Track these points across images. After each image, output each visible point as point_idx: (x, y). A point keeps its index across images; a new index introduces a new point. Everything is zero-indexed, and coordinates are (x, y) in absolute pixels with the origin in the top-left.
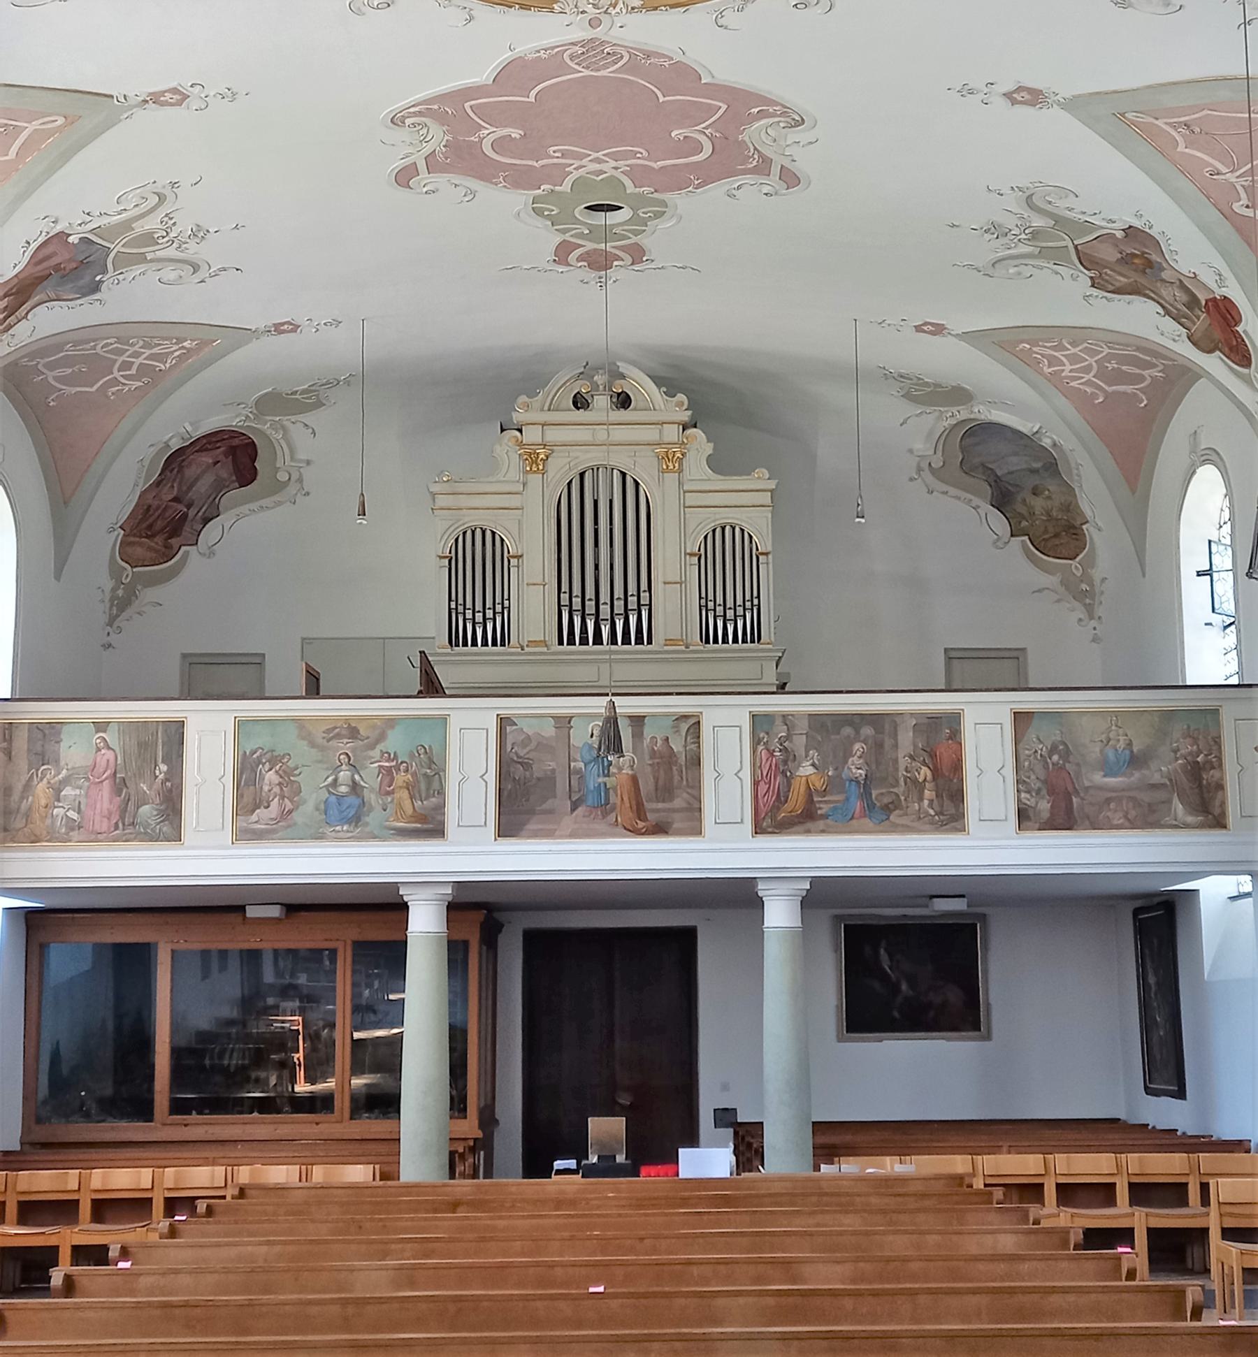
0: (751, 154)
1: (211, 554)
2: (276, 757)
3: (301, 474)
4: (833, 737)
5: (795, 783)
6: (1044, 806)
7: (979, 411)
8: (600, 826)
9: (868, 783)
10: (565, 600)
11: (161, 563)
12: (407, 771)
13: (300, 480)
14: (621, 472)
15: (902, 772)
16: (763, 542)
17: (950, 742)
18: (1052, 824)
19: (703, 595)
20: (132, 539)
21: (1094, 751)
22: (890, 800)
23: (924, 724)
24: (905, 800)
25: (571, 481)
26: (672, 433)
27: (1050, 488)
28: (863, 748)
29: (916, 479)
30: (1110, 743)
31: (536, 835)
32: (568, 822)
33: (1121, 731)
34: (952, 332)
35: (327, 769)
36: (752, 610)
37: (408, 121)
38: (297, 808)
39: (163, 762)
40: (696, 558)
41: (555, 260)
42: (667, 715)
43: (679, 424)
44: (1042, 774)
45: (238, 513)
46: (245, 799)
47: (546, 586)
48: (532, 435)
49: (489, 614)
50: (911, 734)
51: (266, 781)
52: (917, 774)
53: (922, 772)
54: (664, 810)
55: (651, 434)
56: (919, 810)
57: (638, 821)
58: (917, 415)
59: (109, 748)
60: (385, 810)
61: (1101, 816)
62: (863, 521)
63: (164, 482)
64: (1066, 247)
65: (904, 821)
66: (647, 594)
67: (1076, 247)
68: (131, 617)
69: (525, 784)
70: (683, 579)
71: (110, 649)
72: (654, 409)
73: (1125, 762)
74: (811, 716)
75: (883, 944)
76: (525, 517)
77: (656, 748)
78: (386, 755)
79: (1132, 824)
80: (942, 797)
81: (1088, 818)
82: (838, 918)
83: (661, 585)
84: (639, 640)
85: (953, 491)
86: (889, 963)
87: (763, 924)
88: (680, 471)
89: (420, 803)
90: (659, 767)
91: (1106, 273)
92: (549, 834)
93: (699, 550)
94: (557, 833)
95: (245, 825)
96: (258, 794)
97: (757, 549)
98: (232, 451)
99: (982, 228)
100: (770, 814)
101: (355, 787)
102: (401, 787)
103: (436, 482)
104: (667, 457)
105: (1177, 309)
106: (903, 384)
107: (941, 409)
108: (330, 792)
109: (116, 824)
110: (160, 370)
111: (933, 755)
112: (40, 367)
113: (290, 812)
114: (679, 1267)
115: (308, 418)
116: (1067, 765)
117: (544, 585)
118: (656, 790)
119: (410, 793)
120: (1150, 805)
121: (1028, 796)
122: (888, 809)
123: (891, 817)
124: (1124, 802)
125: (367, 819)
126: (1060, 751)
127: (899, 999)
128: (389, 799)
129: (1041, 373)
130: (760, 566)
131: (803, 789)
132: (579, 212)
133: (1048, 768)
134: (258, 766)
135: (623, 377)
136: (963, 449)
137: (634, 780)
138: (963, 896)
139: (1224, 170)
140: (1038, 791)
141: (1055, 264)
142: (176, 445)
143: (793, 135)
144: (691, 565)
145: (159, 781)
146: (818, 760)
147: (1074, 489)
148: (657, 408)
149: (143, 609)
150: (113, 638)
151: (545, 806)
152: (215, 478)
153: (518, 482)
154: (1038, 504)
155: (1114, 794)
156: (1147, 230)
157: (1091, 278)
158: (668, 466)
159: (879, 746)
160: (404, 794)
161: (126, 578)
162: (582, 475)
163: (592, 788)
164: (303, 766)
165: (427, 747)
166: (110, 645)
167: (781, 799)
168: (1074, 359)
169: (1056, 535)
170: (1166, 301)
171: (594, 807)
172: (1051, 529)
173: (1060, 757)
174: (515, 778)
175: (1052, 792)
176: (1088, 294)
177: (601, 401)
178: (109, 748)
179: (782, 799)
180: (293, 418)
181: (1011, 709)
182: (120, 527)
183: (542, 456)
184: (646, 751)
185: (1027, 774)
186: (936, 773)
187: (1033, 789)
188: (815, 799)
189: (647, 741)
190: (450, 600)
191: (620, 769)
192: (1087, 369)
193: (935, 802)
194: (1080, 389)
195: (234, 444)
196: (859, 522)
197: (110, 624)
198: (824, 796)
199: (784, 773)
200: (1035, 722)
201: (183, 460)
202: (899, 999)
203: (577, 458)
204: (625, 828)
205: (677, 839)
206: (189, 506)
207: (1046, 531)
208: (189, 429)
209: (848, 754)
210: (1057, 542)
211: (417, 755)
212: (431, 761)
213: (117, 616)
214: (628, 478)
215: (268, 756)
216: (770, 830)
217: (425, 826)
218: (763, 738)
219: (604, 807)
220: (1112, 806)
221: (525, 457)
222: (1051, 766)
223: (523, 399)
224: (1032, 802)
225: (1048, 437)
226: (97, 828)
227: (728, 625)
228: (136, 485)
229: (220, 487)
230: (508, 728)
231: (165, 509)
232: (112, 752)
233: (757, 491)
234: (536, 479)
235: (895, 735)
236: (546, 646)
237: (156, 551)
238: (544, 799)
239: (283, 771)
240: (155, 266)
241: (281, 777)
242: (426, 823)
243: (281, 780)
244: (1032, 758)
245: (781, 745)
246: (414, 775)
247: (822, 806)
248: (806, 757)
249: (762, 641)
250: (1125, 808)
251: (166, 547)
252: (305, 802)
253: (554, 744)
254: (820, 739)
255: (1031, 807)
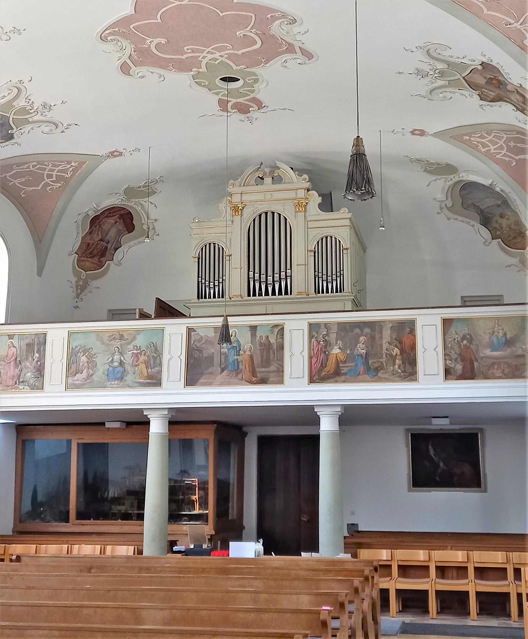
0: (280, 41)
1: (119, 264)
2: (86, 349)
3: (153, 225)
4: (349, 334)
5: (330, 357)
6: (459, 367)
7: (463, 176)
8: (234, 380)
9: (367, 356)
10: (251, 276)
11: (98, 269)
12: (145, 354)
13: (154, 229)
14: (278, 213)
15: (384, 351)
16: (346, 244)
17: (410, 335)
18: (463, 377)
19: (317, 270)
20: (83, 259)
21: (486, 338)
22: (378, 365)
23: (396, 326)
24: (386, 365)
25: (255, 219)
26: (301, 194)
27: (508, 214)
28: (365, 339)
29: (441, 213)
30: (494, 334)
31: (203, 384)
32: (219, 378)
33: (500, 328)
34: (429, 134)
35: (109, 355)
36: (340, 277)
37: (109, 38)
38: (95, 373)
39: (37, 352)
40: (313, 253)
41: (221, 110)
42: (268, 325)
43: (305, 189)
44: (458, 351)
45: (129, 245)
46: (72, 370)
47: (242, 269)
48: (236, 199)
49: (216, 284)
50: (389, 331)
51: (82, 361)
52: (392, 352)
53: (395, 351)
54: (265, 372)
55: (292, 194)
56: (393, 370)
57: (253, 378)
58: (434, 181)
59: (14, 347)
60: (134, 374)
61: (489, 373)
62: (384, 229)
63: (93, 232)
64: (459, 79)
65: (386, 376)
66: (290, 271)
67: (464, 78)
68: (86, 294)
69: (199, 360)
70: (306, 263)
71: (78, 308)
72: (293, 183)
73: (502, 344)
74: (339, 324)
75: (431, 443)
76: (232, 236)
77: (262, 341)
78: (135, 347)
79: (507, 376)
80: (405, 363)
81: (482, 373)
82: (407, 430)
83: (296, 266)
84: (286, 293)
85: (460, 218)
86: (433, 453)
87: (320, 429)
88: (305, 211)
89: (150, 370)
90: (263, 351)
91: (485, 92)
92: (209, 384)
93: (315, 249)
94: (214, 384)
95: (72, 381)
96: (78, 367)
97: (343, 247)
98: (122, 216)
99: (414, 73)
100: (317, 373)
101: (121, 363)
102: (142, 362)
103: (192, 222)
104: (299, 205)
105: (521, 106)
106: (421, 165)
107: (446, 177)
108: (110, 366)
109: (16, 382)
110: (66, 177)
111: (400, 342)
112: (8, 177)
113: (92, 375)
114: (76, 609)
115: (151, 199)
116: (471, 346)
117: (241, 269)
118: (262, 362)
119: (146, 365)
120: (516, 366)
121: (450, 362)
122: (377, 370)
123: (379, 374)
124: (502, 364)
125: (126, 378)
126: (468, 338)
127: (439, 471)
128: (137, 368)
129: (480, 151)
130: (344, 255)
131: (334, 360)
132: (218, 82)
133: (461, 348)
134: (78, 353)
135: (278, 168)
136: (462, 197)
137: (251, 357)
138: (447, 417)
139: (512, 22)
140: (456, 360)
141: (459, 89)
142: (92, 214)
143: (296, 29)
144: (310, 256)
145: (35, 361)
146: (342, 346)
147: (517, 213)
148: (294, 182)
149: (92, 290)
150: (79, 304)
151: (210, 370)
152: (117, 229)
153: (230, 220)
154: (504, 222)
155: (496, 361)
156: (491, 63)
157: (479, 95)
158: (299, 209)
159: (373, 338)
160: (143, 366)
161: (83, 276)
162: (260, 216)
163: (231, 361)
164: (98, 353)
165: (154, 343)
166: (77, 307)
167: (323, 366)
168: (494, 143)
169: (515, 238)
170: (515, 103)
171: (232, 371)
172: (512, 235)
173: (468, 342)
174: (195, 357)
175: (463, 360)
176: (481, 104)
177: (268, 180)
178: (14, 347)
179: (324, 365)
180: (145, 200)
181: (441, 317)
182: (75, 253)
183: (240, 208)
184: (257, 343)
185: (450, 351)
186: (402, 351)
187: (453, 359)
188: (340, 365)
189: (258, 338)
190: (198, 277)
191: (245, 352)
192: (501, 148)
193: (402, 366)
194: (503, 159)
195: (122, 213)
196: (382, 229)
197: (78, 296)
198: (345, 364)
199: (325, 352)
200: (454, 324)
201: (100, 222)
202: (439, 471)
203: (257, 208)
204: (247, 381)
205: (271, 386)
206: (108, 243)
207: (509, 236)
208: (95, 206)
209: (357, 342)
210: (515, 241)
211: (150, 347)
212: (156, 350)
213: (80, 294)
214: (282, 216)
215: (83, 348)
216: (317, 381)
217: (153, 381)
218: (315, 335)
219: (237, 371)
220: (496, 367)
221: (233, 209)
222: (462, 346)
223: (232, 181)
224: (452, 366)
225: (497, 187)
226: (8, 384)
227: (329, 285)
228: (78, 233)
229: (119, 234)
230: (192, 333)
231: (97, 245)
232: (15, 348)
233: (342, 219)
234: (237, 218)
235: (381, 332)
236: (241, 297)
237: (96, 264)
238: (208, 367)
239: (90, 356)
240: (36, 125)
241: (88, 359)
242: (152, 380)
243: (88, 360)
244: (452, 343)
245: (324, 338)
246: (148, 356)
247: (344, 369)
248: (336, 344)
249: (344, 292)
250: (503, 368)
251: (100, 262)
252: (99, 370)
253: (213, 340)
254: (343, 335)
255: (452, 368)
